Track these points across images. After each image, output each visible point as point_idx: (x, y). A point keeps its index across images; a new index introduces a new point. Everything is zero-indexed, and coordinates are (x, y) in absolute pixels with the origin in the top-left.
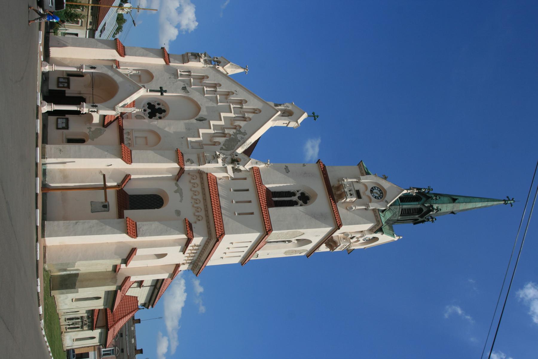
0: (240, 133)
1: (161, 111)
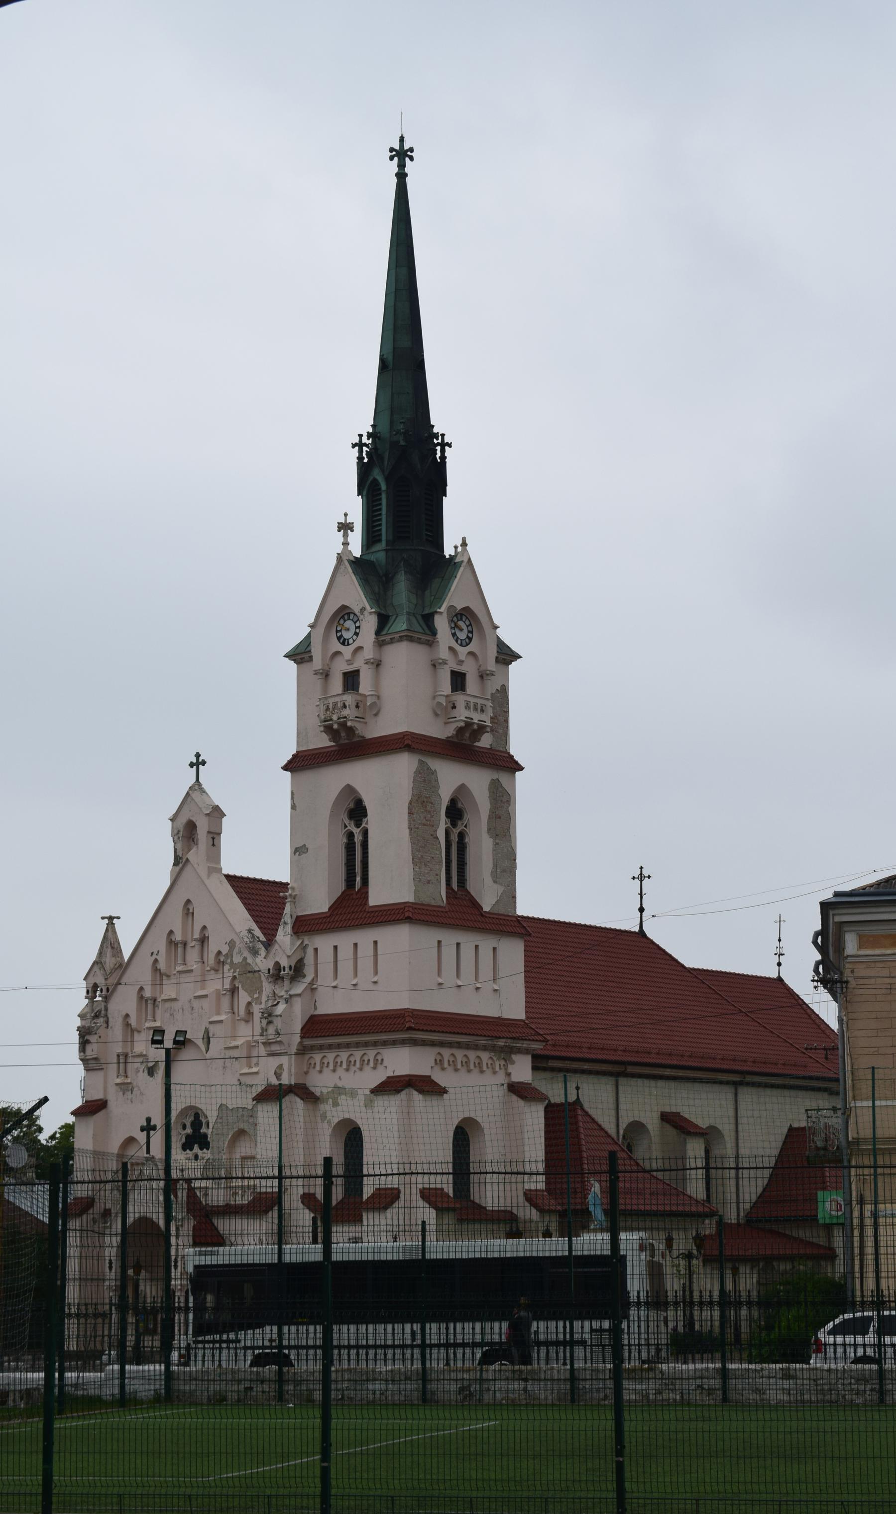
0: (230, 955)
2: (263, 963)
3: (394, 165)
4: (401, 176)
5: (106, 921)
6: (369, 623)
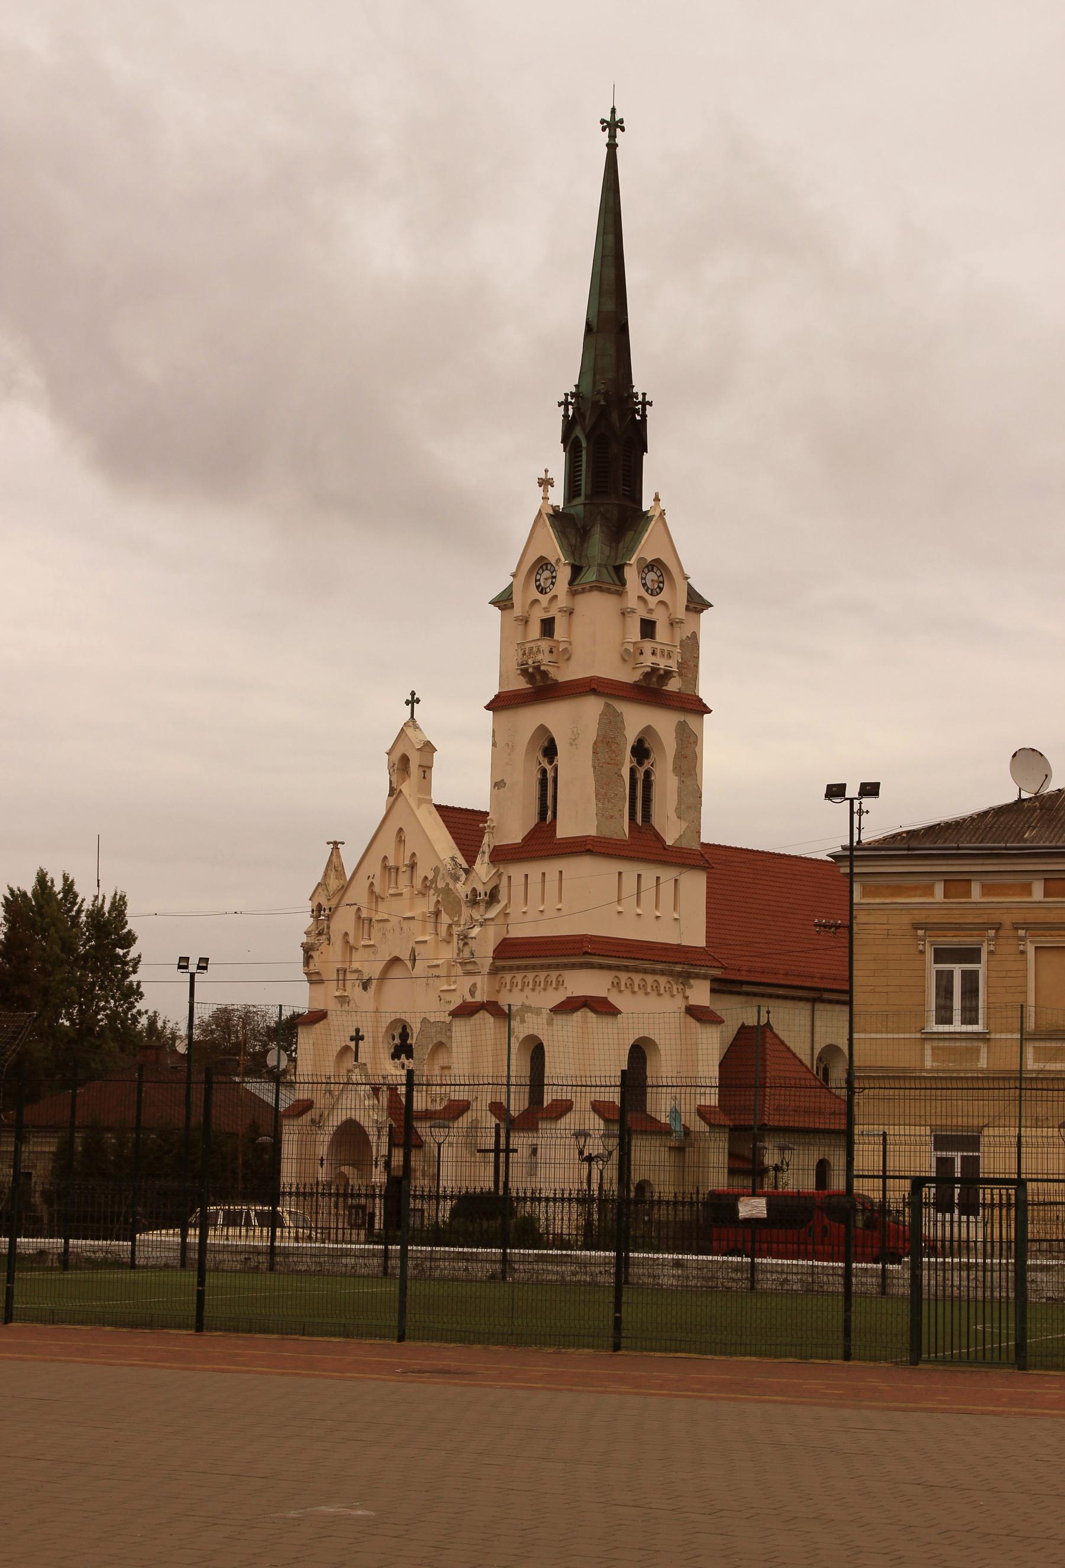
0: (434, 880)
1: (404, 1035)
2: (462, 889)
3: (605, 137)
4: (612, 147)
5: (331, 846)
6: (564, 574)
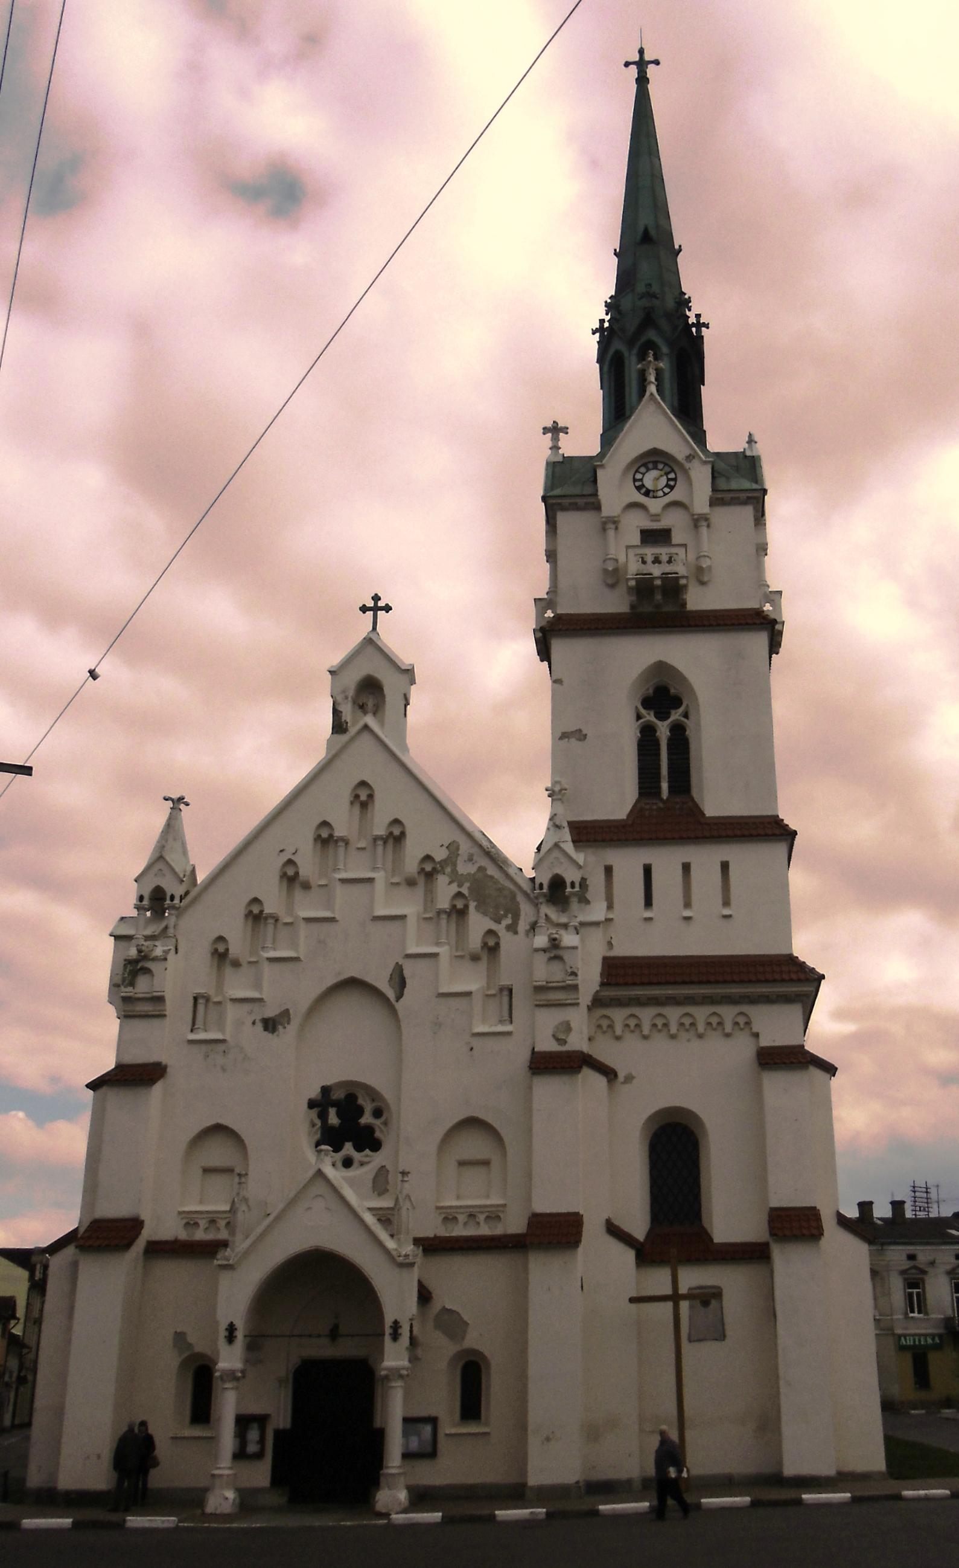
4: (642, 81)
